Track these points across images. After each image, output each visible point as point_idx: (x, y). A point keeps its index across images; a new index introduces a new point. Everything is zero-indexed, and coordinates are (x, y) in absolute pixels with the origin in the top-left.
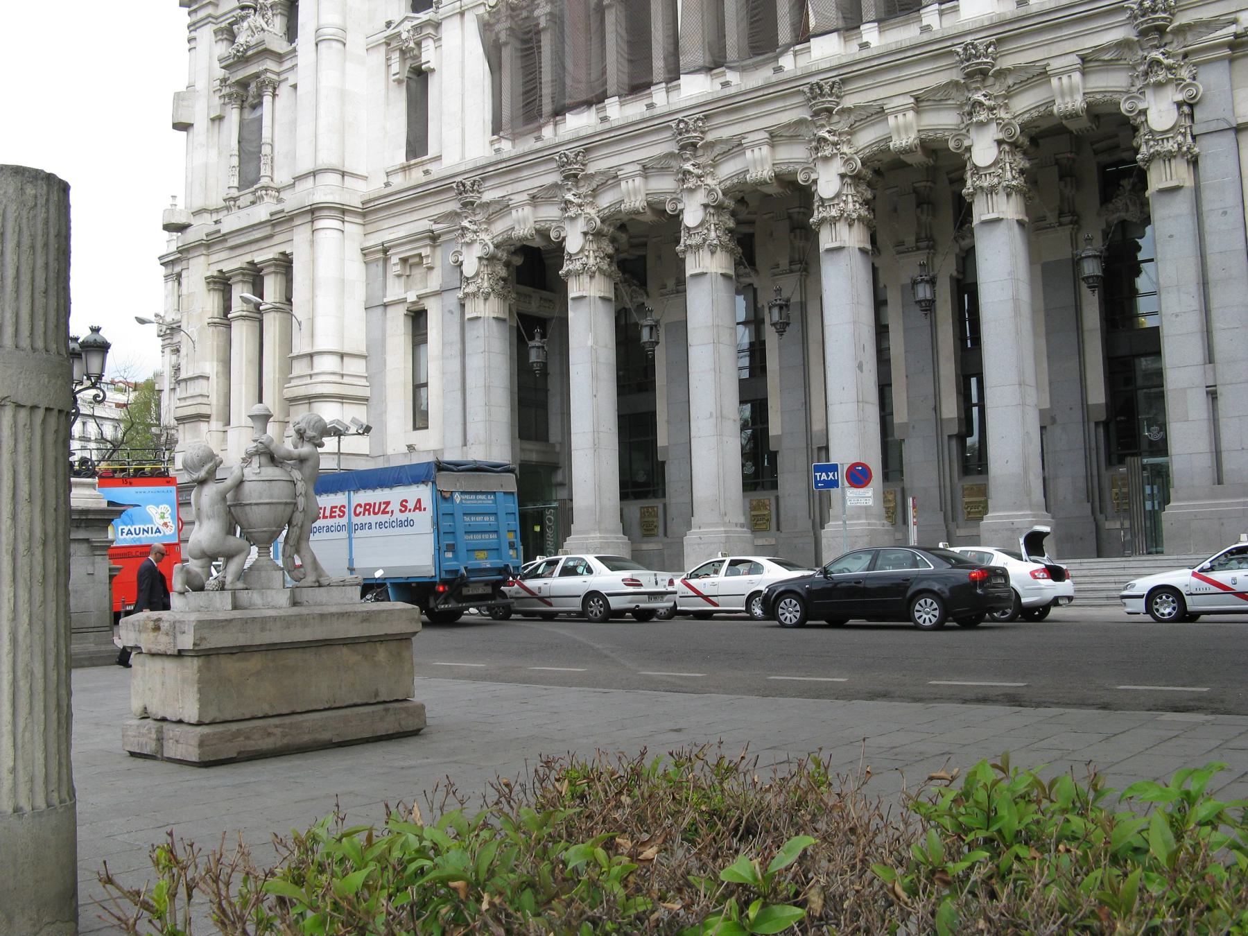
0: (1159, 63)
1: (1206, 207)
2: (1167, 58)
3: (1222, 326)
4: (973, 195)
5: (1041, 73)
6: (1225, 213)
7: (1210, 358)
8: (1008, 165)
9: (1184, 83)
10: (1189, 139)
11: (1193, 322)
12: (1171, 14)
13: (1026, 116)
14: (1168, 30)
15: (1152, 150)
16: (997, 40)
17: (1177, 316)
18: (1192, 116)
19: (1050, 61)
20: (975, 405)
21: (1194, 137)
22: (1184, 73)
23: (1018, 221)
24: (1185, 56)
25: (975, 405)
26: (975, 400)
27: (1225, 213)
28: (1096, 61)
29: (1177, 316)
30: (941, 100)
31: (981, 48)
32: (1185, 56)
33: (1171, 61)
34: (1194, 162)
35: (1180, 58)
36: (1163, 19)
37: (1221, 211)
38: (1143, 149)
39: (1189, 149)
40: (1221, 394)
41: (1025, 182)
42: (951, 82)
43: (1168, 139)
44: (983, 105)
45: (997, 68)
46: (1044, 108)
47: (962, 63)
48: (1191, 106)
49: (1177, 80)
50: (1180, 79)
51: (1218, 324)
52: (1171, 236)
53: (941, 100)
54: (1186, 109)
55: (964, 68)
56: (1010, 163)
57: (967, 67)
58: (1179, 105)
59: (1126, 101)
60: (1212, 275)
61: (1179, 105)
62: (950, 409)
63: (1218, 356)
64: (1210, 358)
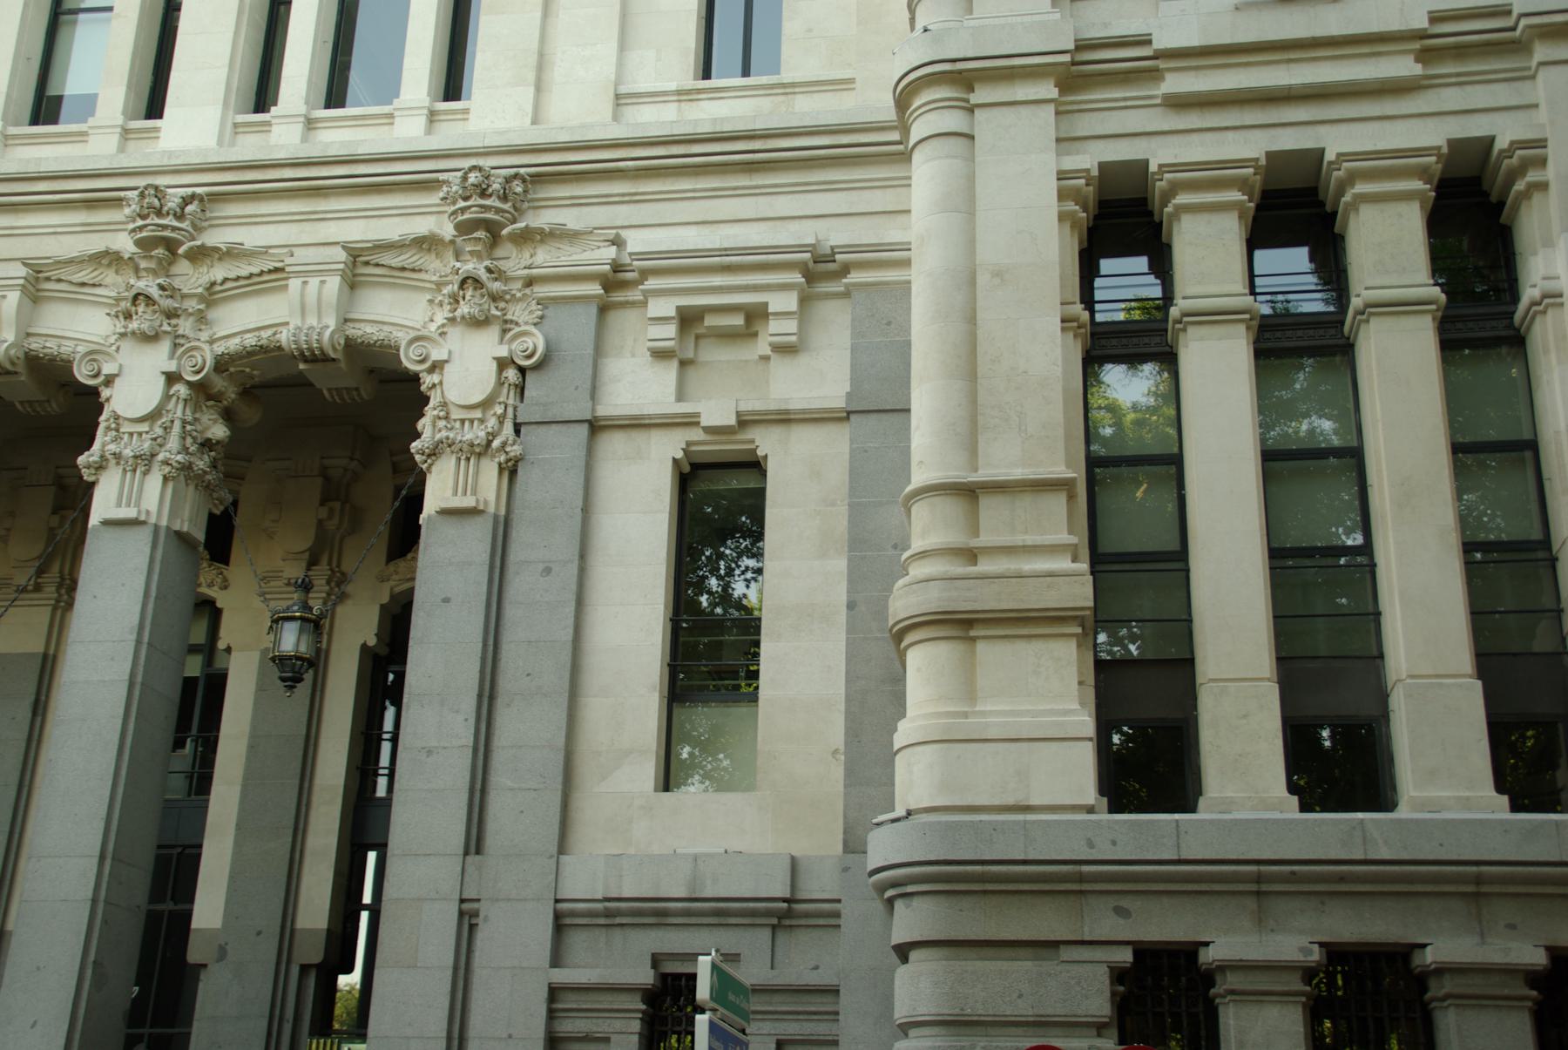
0: (478, 283)
1: (516, 554)
2: (496, 279)
3: (509, 783)
4: (100, 467)
5: (277, 270)
6: (548, 571)
7: (475, 843)
8: (177, 424)
9: (517, 329)
10: (508, 428)
11: (455, 773)
12: (515, 208)
13: (237, 340)
14: (504, 232)
15: (438, 436)
16: (210, 194)
17: (430, 753)
18: (521, 390)
19: (296, 251)
20: (366, 907)
21: (517, 432)
22: (517, 312)
23: (178, 534)
24: (530, 282)
25: (366, 907)
26: (367, 898)
27: (548, 571)
28: (377, 265)
29: (430, 753)
30: (83, 284)
31: (172, 203)
32: (530, 282)
33: (496, 286)
34: (511, 471)
35: (519, 285)
36: (498, 211)
37: (541, 567)
38: (427, 434)
39: (504, 444)
40: (486, 919)
41: (214, 465)
42: (106, 253)
43: (472, 421)
44: (154, 303)
45: (198, 243)
46: (270, 332)
47: (134, 221)
48: (522, 371)
49: (506, 322)
50: (512, 321)
51: (500, 778)
52: (446, 600)
53: (83, 284)
54: (512, 374)
55: (133, 230)
56: (184, 422)
57: (141, 228)
58: (503, 364)
59: (411, 342)
60: (505, 683)
61: (503, 364)
62: (315, 910)
63: (490, 841)
64: (475, 843)
